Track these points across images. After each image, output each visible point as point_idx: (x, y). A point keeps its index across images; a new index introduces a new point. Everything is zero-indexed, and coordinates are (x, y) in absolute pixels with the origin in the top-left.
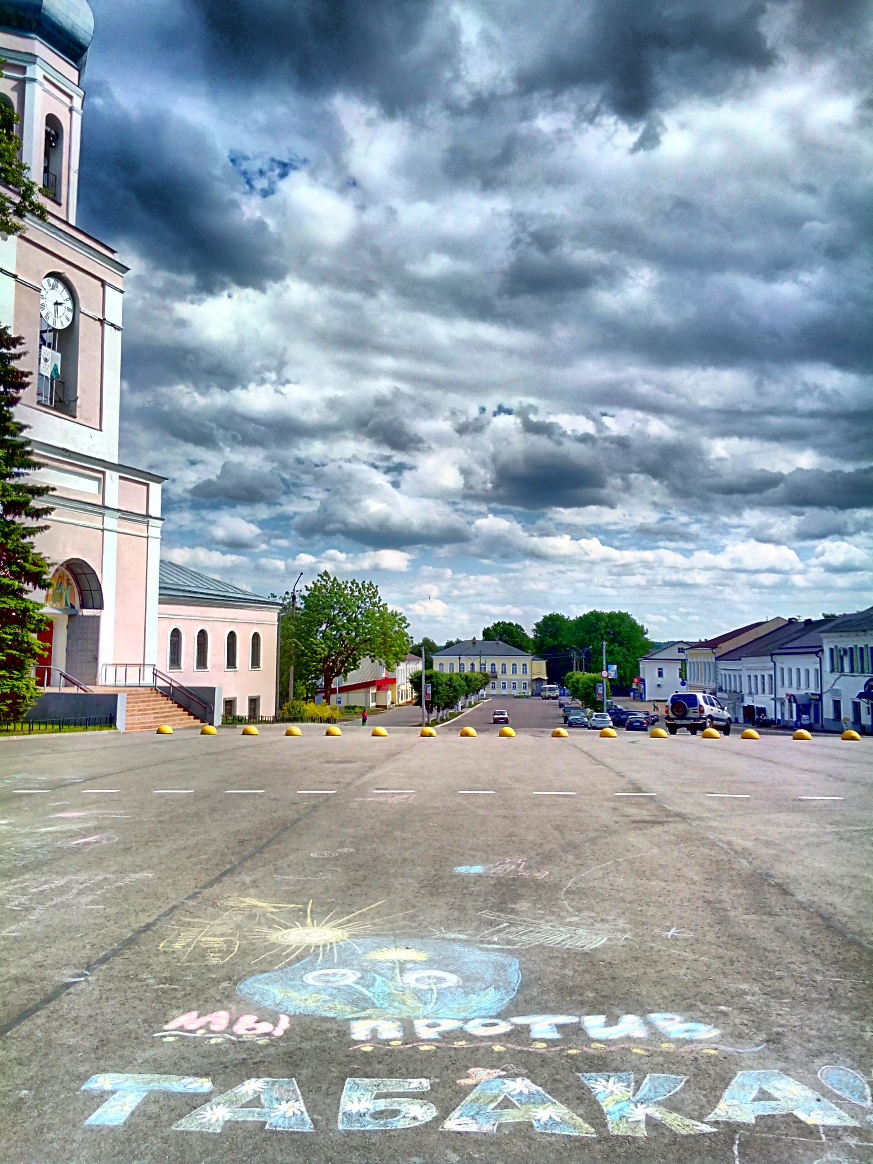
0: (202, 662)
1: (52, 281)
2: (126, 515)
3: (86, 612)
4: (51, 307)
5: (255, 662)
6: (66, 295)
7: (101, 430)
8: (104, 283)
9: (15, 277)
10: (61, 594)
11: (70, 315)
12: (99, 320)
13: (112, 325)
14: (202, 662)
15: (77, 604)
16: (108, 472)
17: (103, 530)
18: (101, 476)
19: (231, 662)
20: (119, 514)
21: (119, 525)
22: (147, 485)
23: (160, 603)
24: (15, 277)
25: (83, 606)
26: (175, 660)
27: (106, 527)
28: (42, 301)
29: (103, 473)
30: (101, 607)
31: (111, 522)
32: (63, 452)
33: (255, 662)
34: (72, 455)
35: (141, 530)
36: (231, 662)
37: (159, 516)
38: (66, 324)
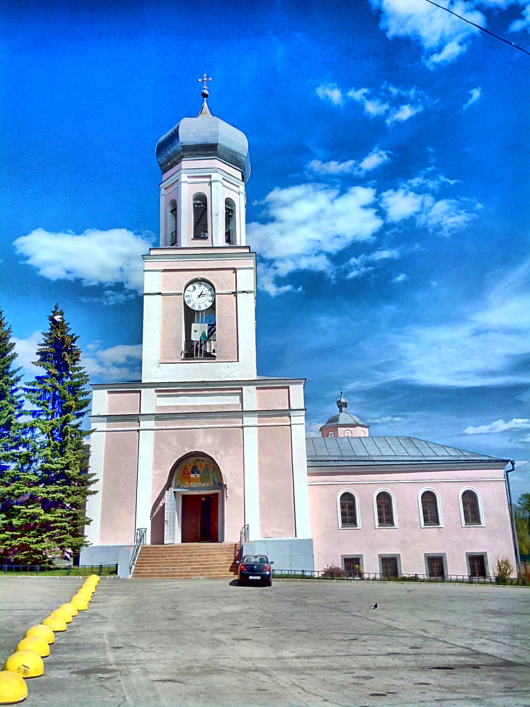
2: (262, 413)
7: (238, 361)
8: (235, 270)
9: (160, 294)
10: (209, 476)
12: (233, 293)
13: (243, 292)
16: (244, 388)
17: (242, 427)
18: (240, 391)
20: (257, 414)
21: (259, 422)
22: (288, 388)
23: (309, 474)
24: (160, 294)
29: (241, 389)
32: (201, 384)
34: (209, 384)
35: (286, 421)
37: (303, 407)
38: (209, 304)
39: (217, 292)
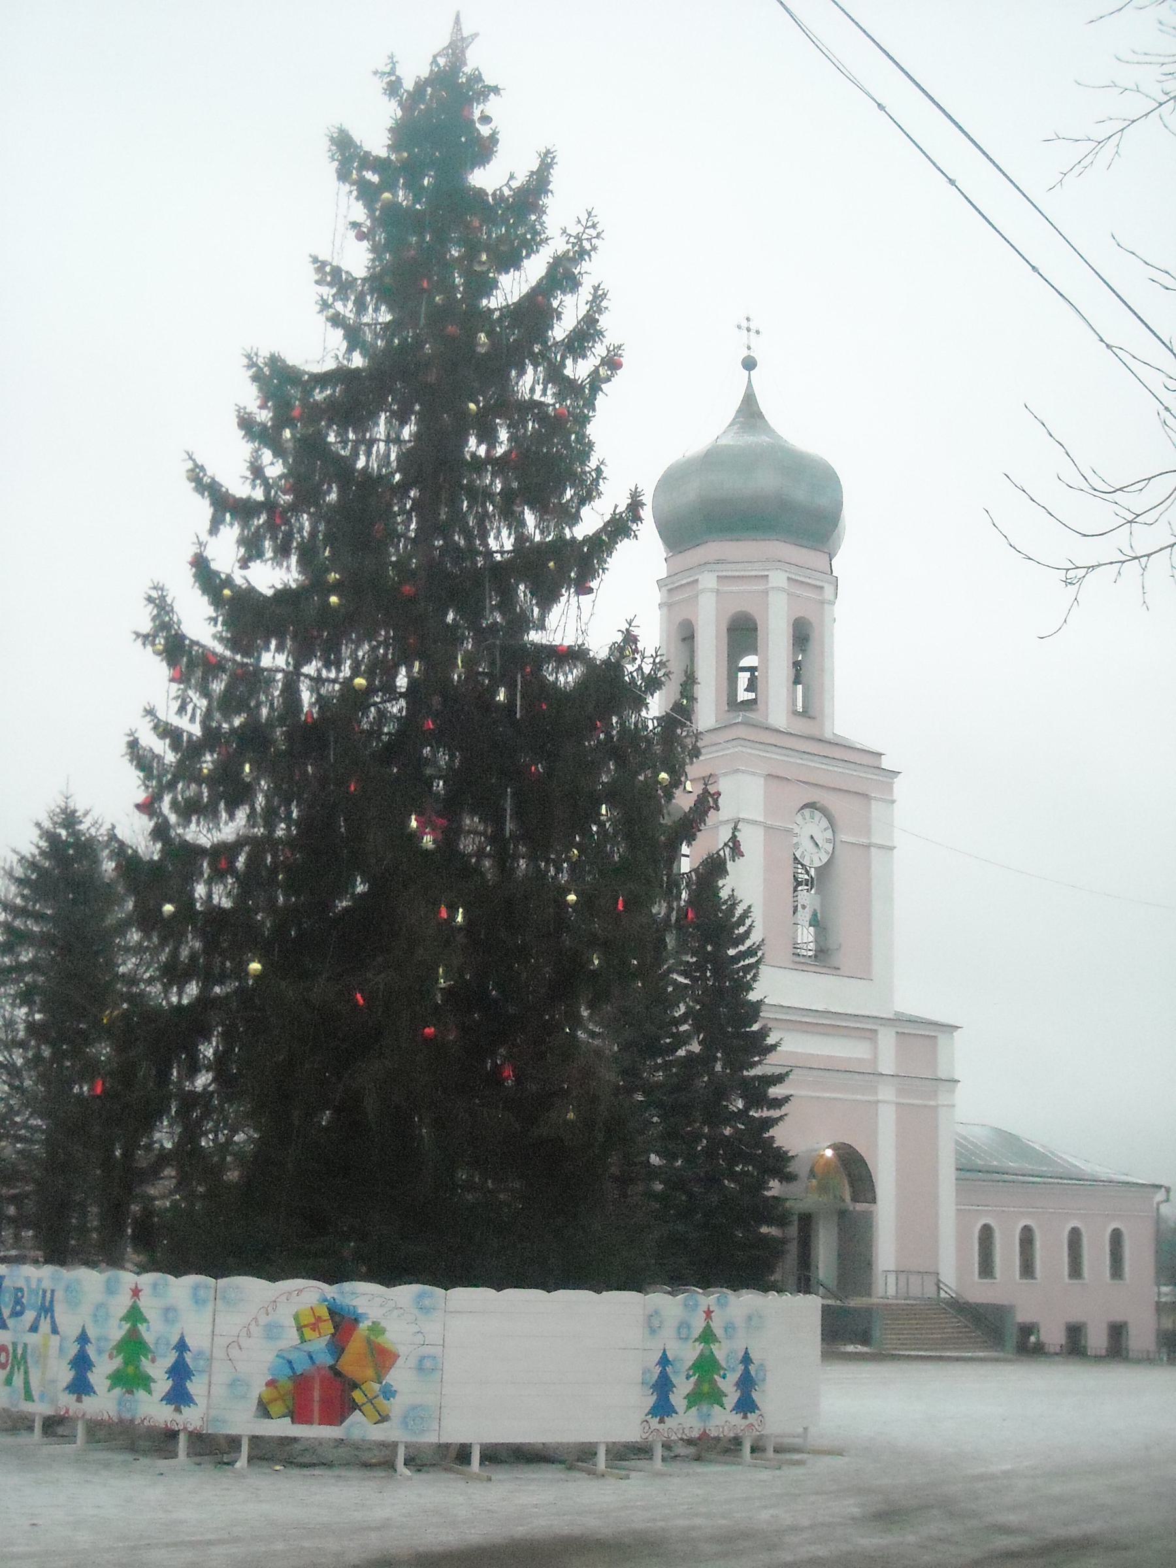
0: (1027, 1269)
1: (807, 812)
3: (860, 1207)
4: (807, 845)
5: (1117, 1269)
6: (825, 823)
11: (829, 847)
14: (1027, 1269)
15: (848, 1198)
19: (1076, 1270)
25: (855, 1199)
26: (986, 1268)
27: (880, 1098)
28: (795, 840)
30: (874, 1201)
31: (887, 1093)
33: (1117, 1269)
36: (1076, 1270)
38: (825, 860)
39: (843, 837)
